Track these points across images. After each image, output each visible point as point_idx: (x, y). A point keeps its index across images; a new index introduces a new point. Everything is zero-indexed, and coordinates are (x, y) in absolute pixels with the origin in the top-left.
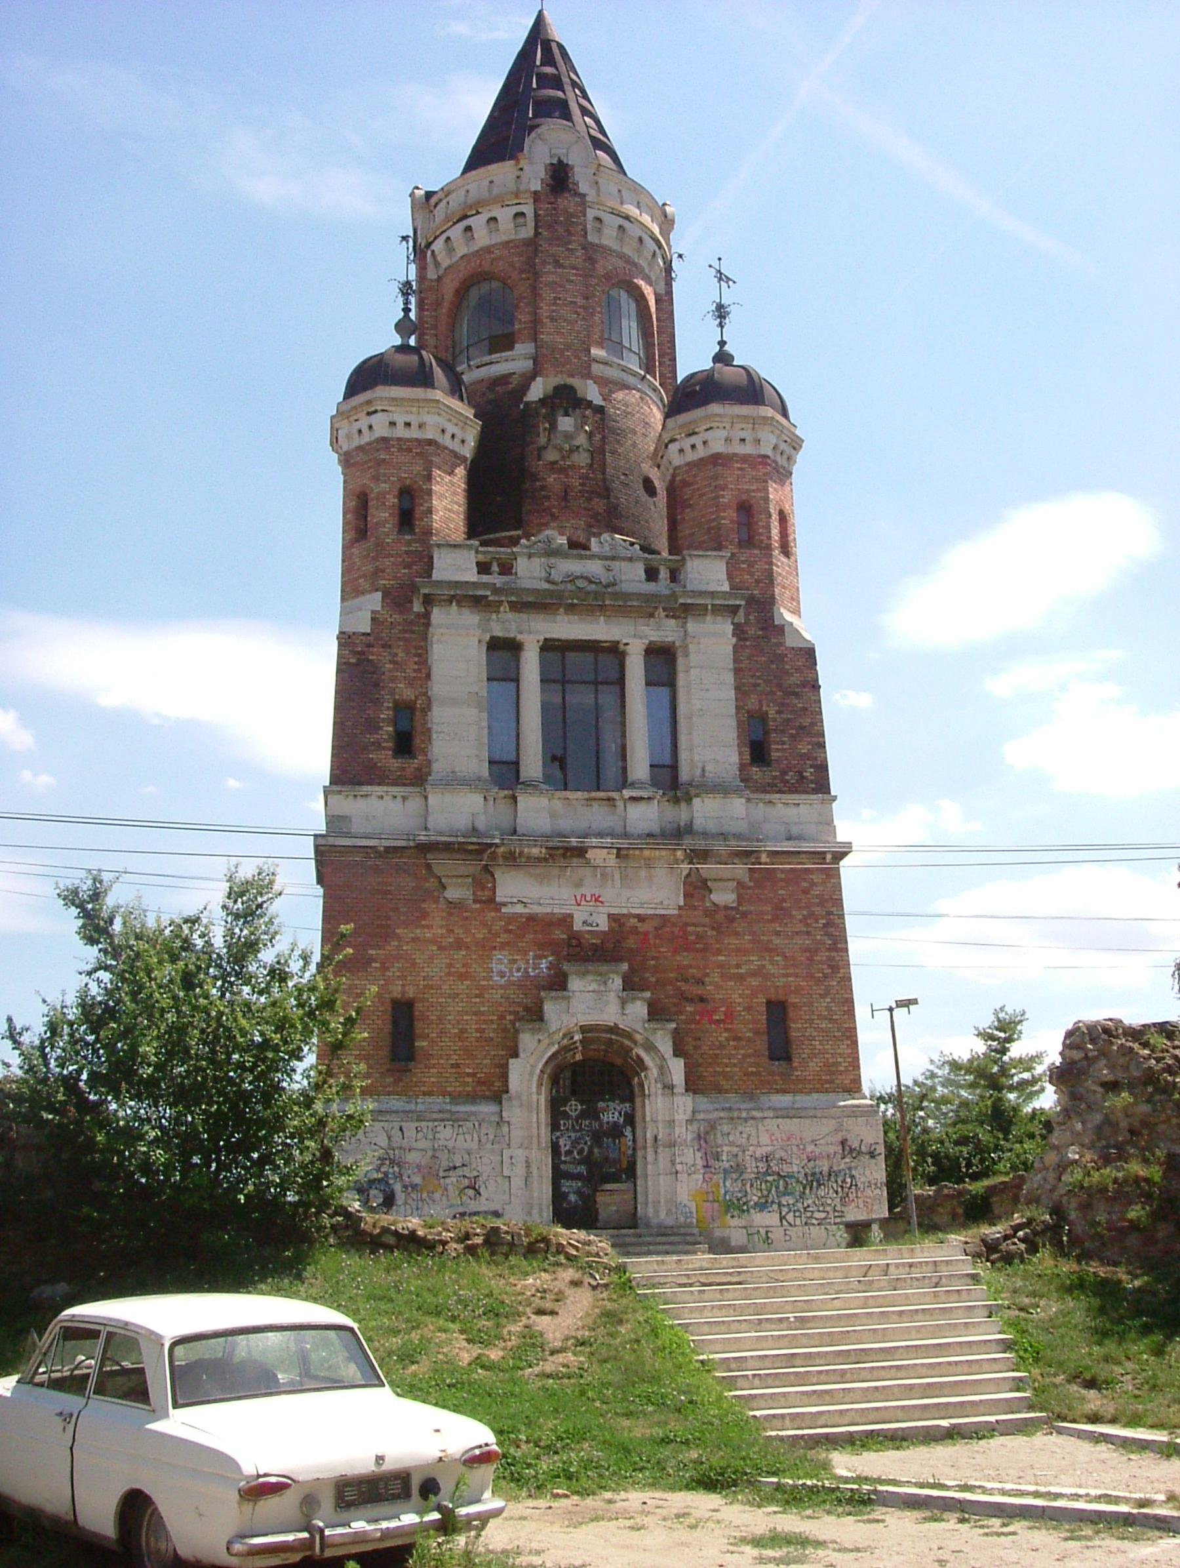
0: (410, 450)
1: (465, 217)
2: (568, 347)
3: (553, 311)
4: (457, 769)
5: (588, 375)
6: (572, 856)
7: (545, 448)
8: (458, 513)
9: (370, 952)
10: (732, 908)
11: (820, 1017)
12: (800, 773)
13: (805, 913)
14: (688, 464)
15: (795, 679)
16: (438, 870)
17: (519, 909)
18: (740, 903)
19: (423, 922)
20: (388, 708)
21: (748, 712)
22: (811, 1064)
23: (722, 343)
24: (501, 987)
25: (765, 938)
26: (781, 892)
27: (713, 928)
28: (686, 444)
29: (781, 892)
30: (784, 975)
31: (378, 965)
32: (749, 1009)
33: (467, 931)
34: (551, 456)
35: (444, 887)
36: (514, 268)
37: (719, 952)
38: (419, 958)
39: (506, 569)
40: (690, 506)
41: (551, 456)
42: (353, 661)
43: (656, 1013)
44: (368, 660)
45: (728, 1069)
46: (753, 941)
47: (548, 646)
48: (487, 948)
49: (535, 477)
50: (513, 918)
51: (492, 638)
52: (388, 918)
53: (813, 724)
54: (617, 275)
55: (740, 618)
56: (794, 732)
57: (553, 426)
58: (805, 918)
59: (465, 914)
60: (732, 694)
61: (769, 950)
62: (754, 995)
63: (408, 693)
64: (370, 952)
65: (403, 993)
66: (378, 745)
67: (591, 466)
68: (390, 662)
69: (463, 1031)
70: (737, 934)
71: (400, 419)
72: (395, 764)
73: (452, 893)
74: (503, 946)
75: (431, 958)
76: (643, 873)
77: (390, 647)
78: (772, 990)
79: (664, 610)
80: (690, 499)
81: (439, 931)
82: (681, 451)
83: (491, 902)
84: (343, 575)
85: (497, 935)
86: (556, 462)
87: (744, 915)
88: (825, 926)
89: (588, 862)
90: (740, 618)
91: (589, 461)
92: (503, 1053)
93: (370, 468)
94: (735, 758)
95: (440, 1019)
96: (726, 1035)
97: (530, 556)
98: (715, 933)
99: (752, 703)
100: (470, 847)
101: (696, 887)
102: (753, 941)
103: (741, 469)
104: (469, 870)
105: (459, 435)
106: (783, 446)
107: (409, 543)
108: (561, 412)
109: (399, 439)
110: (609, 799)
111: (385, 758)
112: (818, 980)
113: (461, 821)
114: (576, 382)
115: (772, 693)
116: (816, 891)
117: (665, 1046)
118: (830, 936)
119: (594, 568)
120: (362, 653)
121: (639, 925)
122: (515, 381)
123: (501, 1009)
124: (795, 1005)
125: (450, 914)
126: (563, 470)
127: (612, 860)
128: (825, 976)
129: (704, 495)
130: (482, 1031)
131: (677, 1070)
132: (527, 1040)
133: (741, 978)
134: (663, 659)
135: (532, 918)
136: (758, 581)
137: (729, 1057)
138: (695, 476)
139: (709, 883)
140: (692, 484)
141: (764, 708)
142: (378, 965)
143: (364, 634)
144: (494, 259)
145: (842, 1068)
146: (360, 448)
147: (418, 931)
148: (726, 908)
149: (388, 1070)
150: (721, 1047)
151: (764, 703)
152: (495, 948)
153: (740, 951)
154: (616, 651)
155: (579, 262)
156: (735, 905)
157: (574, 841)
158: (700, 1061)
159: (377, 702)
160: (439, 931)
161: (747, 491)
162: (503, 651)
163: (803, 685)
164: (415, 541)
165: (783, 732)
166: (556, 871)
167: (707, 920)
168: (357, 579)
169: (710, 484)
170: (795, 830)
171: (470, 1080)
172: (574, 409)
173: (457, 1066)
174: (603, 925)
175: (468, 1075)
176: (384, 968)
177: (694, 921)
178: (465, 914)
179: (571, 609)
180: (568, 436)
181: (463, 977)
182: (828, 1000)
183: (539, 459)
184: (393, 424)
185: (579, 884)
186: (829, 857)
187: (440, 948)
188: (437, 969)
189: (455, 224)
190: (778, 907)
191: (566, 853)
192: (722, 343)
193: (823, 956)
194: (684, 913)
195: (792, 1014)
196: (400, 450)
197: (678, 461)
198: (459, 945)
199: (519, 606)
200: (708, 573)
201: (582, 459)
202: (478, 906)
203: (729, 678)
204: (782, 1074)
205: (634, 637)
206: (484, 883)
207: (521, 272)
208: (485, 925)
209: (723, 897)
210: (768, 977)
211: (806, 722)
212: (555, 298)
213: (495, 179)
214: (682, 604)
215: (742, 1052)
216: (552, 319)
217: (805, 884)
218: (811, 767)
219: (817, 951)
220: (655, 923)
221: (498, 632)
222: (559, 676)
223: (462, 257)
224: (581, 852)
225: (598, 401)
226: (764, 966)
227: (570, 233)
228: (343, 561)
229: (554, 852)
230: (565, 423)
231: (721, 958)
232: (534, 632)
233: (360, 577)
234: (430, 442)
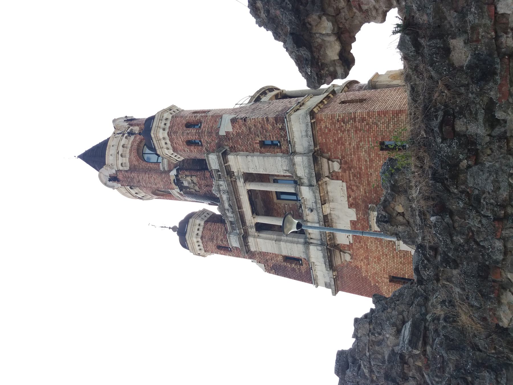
10: (341, 162)
18: (338, 158)
24: (382, 248)
58: (341, 131)
69: (401, 263)
89: (330, 214)
101: (334, 176)
148: (341, 163)
162: (260, 228)
167: (347, 171)
177: (348, 176)
194: (345, 181)
209: (336, 166)
232: (251, 220)
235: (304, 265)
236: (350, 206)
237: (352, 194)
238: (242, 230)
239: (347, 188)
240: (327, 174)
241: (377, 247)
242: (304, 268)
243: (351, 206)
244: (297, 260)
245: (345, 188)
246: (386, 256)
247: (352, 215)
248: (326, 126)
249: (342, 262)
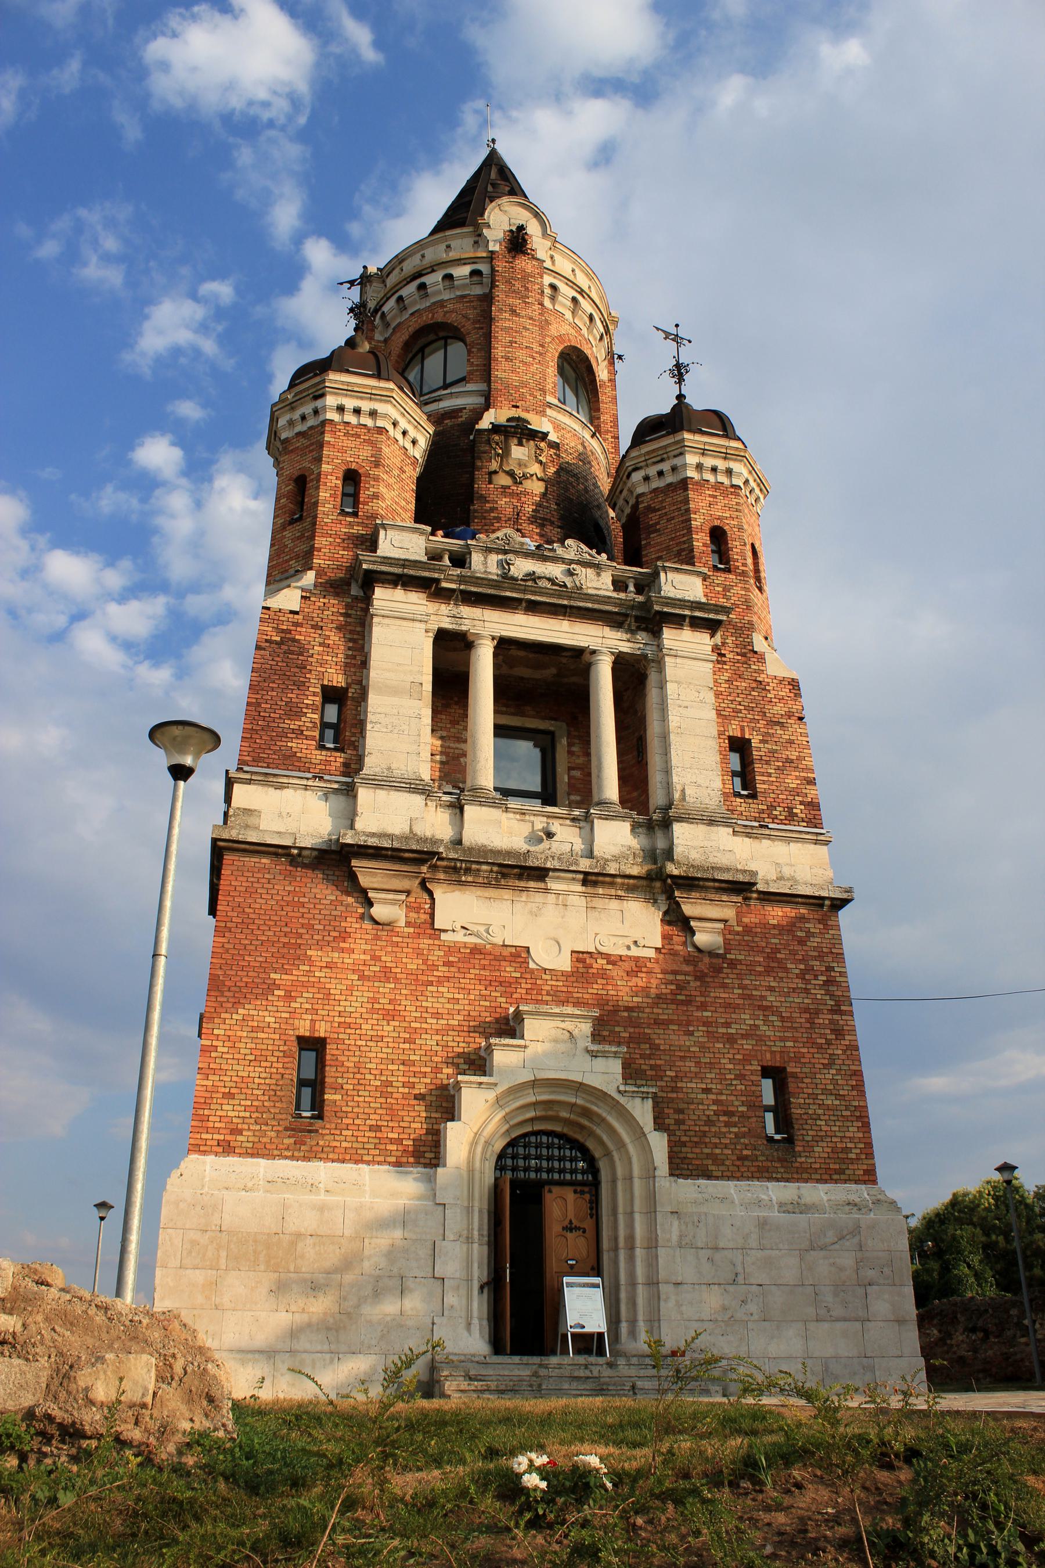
0: (359, 436)
1: (419, 275)
2: (524, 384)
3: (509, 352)
4: (393, 766)
5: (543, 413)
6: (530, 878)
7: (495, 472)
9: (273, 976)
10: (718, 955)
11: (826, 1092)
12: (790, 809)
13: (802, 967)
14: (655, 490)
15: (779, 709)
16: (364, 881)
18: (728, 951)
19: (342, 945)
20: (314, 694)
21: (730, 738)
22: (816, 1149)
23: (680, 397)
25: (758, 993)
26: (773, 941)
27: (697, 978)
28: (652, 471)
29: (773, 941)
30: (783, 1039)
31: (282, 993)
32: (741, 1077)
33: (398, 961)
35: (370, 904)
36: (469, 319)
37: (703, 1007)
38: (336, 988)
39: (460, 560)
40: (658, 531)
41: (503, 480)
42: (278, 639)
43: (631, 1073)
44: (294, 640)
45: (718, 1151)
46: (742, 996)
47: (504, 646)
48: (420, 983)
49: (484, 499)
52: (300, 936)
54: (569, 340)
55: (718, 639)
56: (780, 764)
57: (507, 452)
59: (395, 939)
60: (713, 714)
61: (761, 1008)
62: (746, 1060)
63: (337, 679)
64: (273, 976)
65: (313, 1028)
66: (299, 733)
67: (544, 495)
68: (320, 645)
70: (724, 986)
72: (319, 756)
74: (440, 983)
75: (350, 989)
76: (614, 904)
77: (321, 628)
78: (768, 1056)
79: (637, 619)
80: (658, 523)
81: (363, 957)
82: (647, 478)
83: (429, 927)
84: (270, 560)
85: (434, 967)
86: (509, 487)
87: (733, 964)
88: (826, 983)
91: (543, 490)
92: (438, 1115)
93: (311, 451)
94: (718, 784)
95: (358, 1066)
96: (715, 1108)
98: (698, 983)
99: (734, 730)
100: (407, 855)
102: (742, 996)
103: (715, 497)
105: (412, 433)
107: (351, 525)
108: (516, 441)
111: (306, 748)
112: (820, 1047)
115: (752, 720)
116: (814, 942)
117: (643, 1112)
118: (832, 996)
119: (555, 570)
120: (289, 632)
121: (610, 967)
122: (464, 417)
123: (436, 1059)
124: (794, 1075)
125: (377, 938)
126: (518, 495)
128: (829, 1043)
129: (673, 518)
130: (413, 1086)
131: (659, 1144)
133: (731, 1039)
135: (476, 951)
137: (719, 1135)
138: (662, 502)
139: (692, 923)
140: (658, 510)
141: (747, 737)
142: (282, 993)
143: (292, 612)
144: (447, 312)
145: (853, 1156)
146: (299, 434)
147: (336, 955)
148: (711, 954)
149: (286, 1129)
150: (709, 1122)
151: (746, 729)
152: (431, 983)
153: (729, 1006)
155: (535, 315)
156: (721, 951)
158: (684, 1139)
159: (302, 686)
160: (363, 957)
163: (789, 715)
164: (358, 524)
165: (767, 763)
166: (507, 894)
168: (287, 561)
169: (679, 509)
170: (787, 872)
171: (394, 1147)
172: (528, 440)
173: (377, 1128)
175: (392, 1141)
176: (289, 997)
178: (395, 939)
179: (533, 608)
180: (521, 464)
181: (390, 1016)
182: (834, 1072)
183: (490, 482)
186: (827, 902)
187: (362, 977)
188: (356, 1004)
189: (408, 283)
190: (772, 956)
191: (520, 873)
192: (680, 397)
193: (824, 1019)
195: (792, 1086)
196: (346, 434)
197: (641, 489)
198: (386, 975)
202: (411, 930)
203: (710, 697)
204: (780, 1160)
207: (474, 322)
208: (419, 953)
210: (761, 1039)
211: (794, 755)
212: (511, 342)
213: (453, 244)
214: (658, 612)
215: (736, 1130)
216: (507, 359)
217: (799, 934)
218: (801, 803)
219: (817, 1012)
220: (627, 966)
221: (447, 624)
223: (412, 314)
225: (553, 437)
226: (757, 1027)
227: (527, 289)
228: (272, 545)
229: (505, 870)
230: (518, 452)
231: (705, 1014)
232: (490, 625)
233: (291, 559)
234: (381, 430)
236: (580, 957)
237: (615, 972)
238: (453, 586)
239: (637, 959)
240: (688, 909)
241: (437, 1015)
243: (578, 960)
245: (635, 952)
246: (410, 1041)
247: (551, 957)
248: (813, 935)
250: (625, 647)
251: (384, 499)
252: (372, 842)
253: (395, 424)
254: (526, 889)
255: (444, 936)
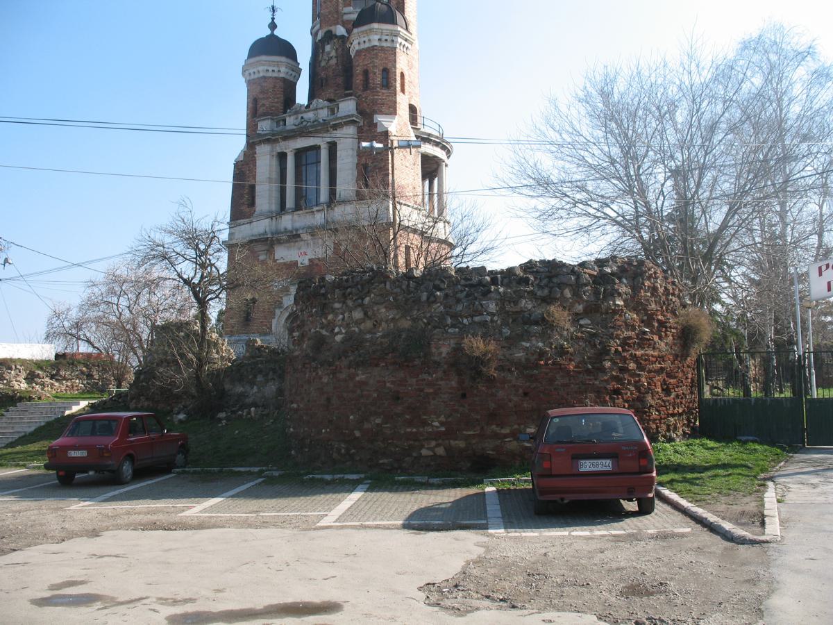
8: (277, 103)
17: (282, 261)
21: (363, 165)
34: (323, 64)
50: (281, 263)
51: (278, 153)
53: (385, 165)
67: (336, 64)
71: (251, 71)
73: (262, 257)
90: (362, 124)
97: (290, 116)
104: (266, 247)
106: (384, 37)
108: (326, 43)
109: (253, 79)
110: (312, 212)
113: (261, 230)
114: (332, 28)
127: (309, 237)
132: (278, 312)
134: (333, 148)
135: (285, 264)
136: (369, 105)
154: (316, 148)
157: (294, 233)
161: (366, 65)
162: (282, 157)
166: (292, 244)
173: (262, 322)
174: (307, 263)
180: (329, 53)
184: (250, 74)
185: (299, 249)
199: (285, 138)
200: (348, 107)
201: (333, 62)
205: (321, 141)
206: (270, 251)
222: (308, 162)
224: (299, 236)
232: (291, 147)
234: (264, 77)
235: (248, 210)
236: (310, 260)
242: (245, 208)
244: (252, 203)
249: (256, 252)
250: (329, 140)
251: (264, 105)
252: (253, 238)
253: (267, 71)
254: (296, 241)
255: (278, 261)
